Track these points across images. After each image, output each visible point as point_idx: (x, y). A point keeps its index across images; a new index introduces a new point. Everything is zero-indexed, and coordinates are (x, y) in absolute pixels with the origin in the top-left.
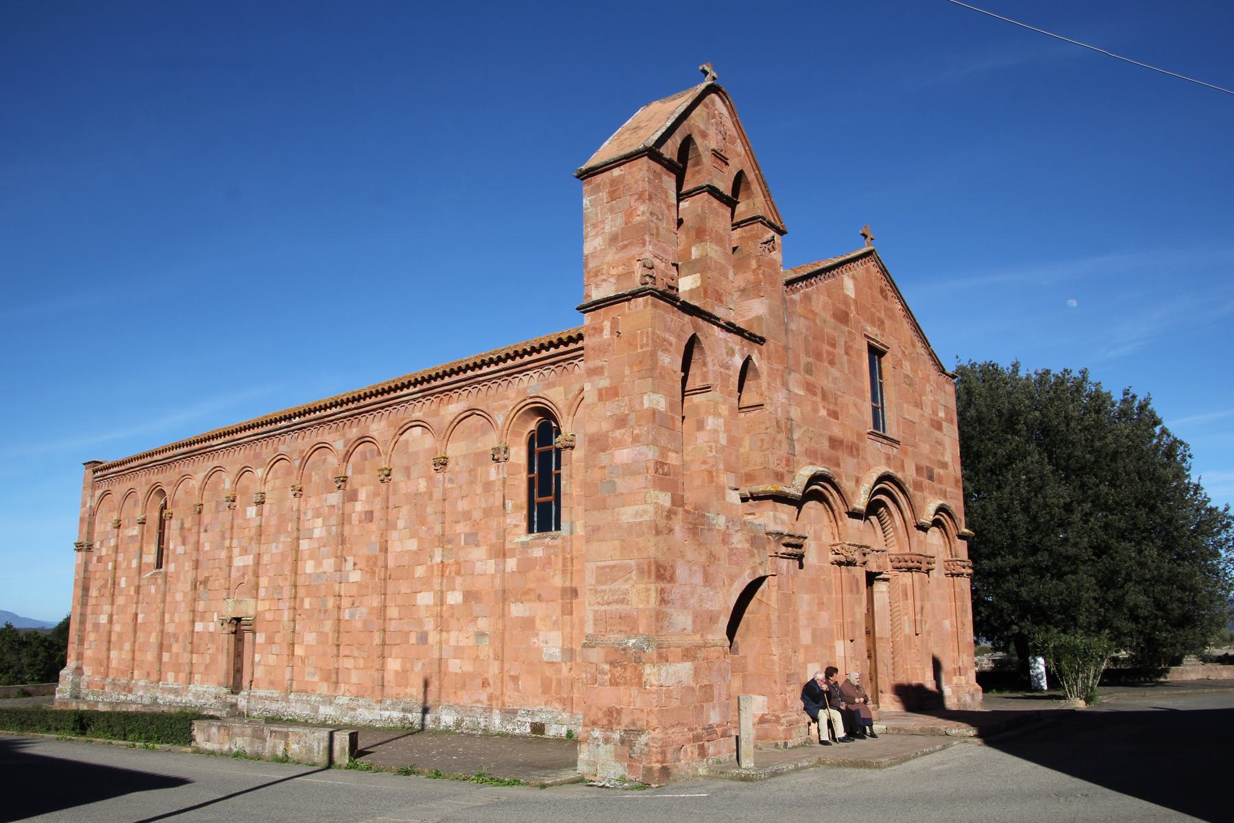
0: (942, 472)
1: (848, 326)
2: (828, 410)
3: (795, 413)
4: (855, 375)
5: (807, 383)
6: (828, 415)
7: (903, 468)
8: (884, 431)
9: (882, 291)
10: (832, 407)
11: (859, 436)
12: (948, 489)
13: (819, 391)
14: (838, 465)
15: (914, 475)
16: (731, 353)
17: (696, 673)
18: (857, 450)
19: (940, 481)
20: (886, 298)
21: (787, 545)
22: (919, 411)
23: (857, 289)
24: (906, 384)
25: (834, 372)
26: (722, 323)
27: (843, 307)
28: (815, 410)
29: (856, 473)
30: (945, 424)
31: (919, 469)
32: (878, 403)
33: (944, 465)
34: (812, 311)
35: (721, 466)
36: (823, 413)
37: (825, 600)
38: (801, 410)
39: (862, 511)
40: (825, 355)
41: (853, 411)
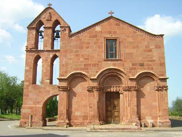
0: (150, 63)
1: (96, 37)
2: (84, 59)
3: (69, 61)
4: (99, 48)
5: (75, 55)
6: (84, 59)
7: (123, 65)
8: (116, 57)
9: (116, 24)
10: (86, 57)
11: (99, 62)
12: (154, 67)
13: (81, 56)
14: (88, 69)
15: (131, 66)
16: (50, 55)
17: (32, 112)
18: (98, 65)
19: (148, 65)
20: (119, 25)
21: (61, 88)
22: (136, 49)
23: (102, 29)
24: (128, 44)
25: (88, 50)
26: (45, 50)
27: (95, 34)
28: (79, 59)
29: (97, 70)
30: (153, 50)
31: (133, 65)
32: (113, 51)
33: (154, 61)
34: (80, 39)
35: (44, 76)
36: (82, 59)
37: (84, 99)
38: (73, 61)
39: (95, 79)
40: (84, 47)
41: (96, 56)
